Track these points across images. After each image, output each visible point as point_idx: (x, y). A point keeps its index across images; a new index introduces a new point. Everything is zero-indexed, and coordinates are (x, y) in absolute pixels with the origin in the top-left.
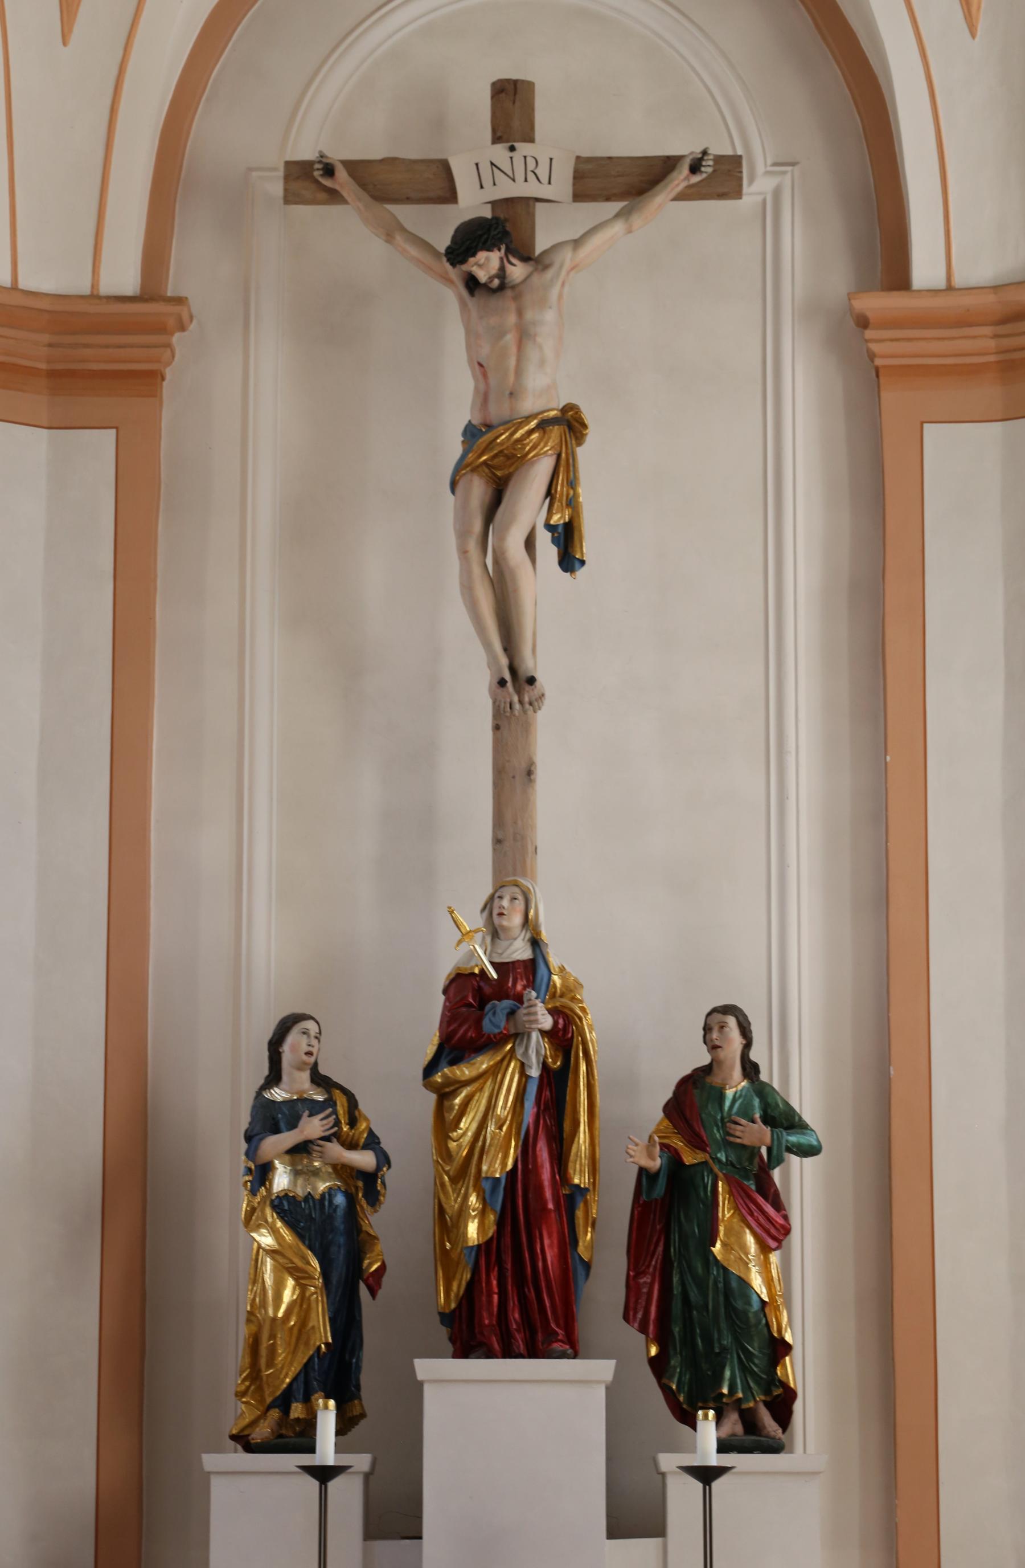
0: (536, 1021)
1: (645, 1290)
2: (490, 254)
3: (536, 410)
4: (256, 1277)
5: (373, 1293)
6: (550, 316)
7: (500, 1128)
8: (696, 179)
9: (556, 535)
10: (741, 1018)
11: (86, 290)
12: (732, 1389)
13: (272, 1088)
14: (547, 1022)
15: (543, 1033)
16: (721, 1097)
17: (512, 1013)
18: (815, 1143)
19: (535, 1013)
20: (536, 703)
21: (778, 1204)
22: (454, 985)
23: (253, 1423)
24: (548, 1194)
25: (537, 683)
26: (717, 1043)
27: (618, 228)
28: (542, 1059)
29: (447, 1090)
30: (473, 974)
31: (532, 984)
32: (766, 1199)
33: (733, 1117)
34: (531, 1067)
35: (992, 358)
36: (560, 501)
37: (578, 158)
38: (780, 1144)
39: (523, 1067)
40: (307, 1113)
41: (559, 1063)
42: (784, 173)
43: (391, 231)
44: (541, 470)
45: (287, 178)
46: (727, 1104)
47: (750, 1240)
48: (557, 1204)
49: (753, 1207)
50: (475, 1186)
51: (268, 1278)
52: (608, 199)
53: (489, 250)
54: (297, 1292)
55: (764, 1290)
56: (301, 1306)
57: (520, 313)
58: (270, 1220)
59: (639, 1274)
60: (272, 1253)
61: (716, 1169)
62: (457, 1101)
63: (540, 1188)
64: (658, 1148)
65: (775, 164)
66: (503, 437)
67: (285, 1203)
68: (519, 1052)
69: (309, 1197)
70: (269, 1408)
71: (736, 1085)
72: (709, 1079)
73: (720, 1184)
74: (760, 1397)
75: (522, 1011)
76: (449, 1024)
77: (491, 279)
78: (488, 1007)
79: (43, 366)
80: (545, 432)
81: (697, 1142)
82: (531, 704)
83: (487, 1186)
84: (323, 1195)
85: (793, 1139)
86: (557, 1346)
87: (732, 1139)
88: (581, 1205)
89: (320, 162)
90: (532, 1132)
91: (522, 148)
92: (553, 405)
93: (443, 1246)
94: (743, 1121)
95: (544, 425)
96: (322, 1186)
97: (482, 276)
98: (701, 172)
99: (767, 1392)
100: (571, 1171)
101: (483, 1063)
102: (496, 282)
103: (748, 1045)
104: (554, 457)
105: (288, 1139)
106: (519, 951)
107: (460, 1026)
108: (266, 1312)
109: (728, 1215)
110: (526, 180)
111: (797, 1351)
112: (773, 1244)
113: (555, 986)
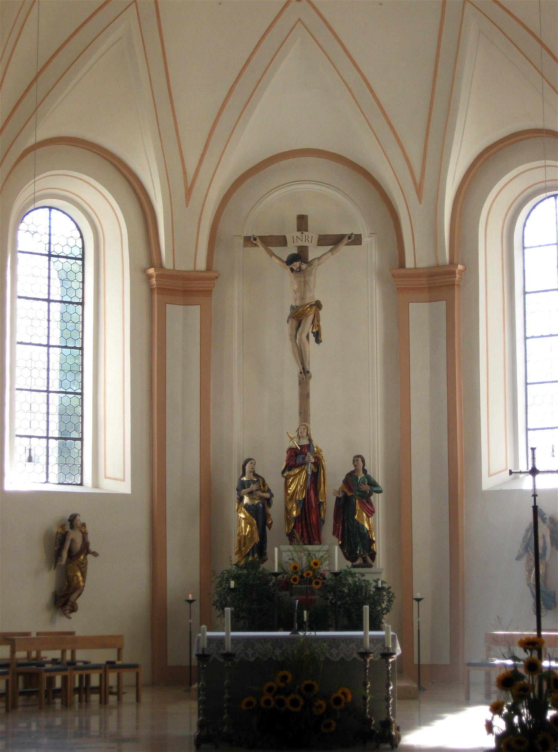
0: (310, 460)
1: (338, 527)
2: (297, 263)
3: (309, 302)
4: (240, 525)
5: (270, 528)
6: (312, 278)
7: (301, 488)
8: (350, 240)
9: (314, 334)
11: (193, 270)
12: (360, 552)
13: (243, 477)
14: (313, 460)
15: (312, 463)
16: (357, 478)
17: (304, 458)
18: (381, 490)
19: (310, 458)
20: (310, 377)
21: (371, 505)
22: (289, 451)
23: (239, 562)
24: (314, 504)
25: (310, 373)
26: (356, 465)
27: (330, 254)
28: (312, 470)
29: (288, 477)
30: (294, 448)
31: (309, 450)
32: (369, 504)
33: (360, 484)
34: (309, 472)
35: (426, 286)
36: (315, 325)
37: (319, 235)
38: (372, 491)
39: (307, 472)
40: (252, 484)
41: (316, 471)
42: (373, 236)
43: (272, 254)
44: (311, 318)
45: (245, 241)
46: (358, 481)
47: (365, 515)
48: (316, 506)
49: (365, 506)
50: (295, 502)
51: (243, 525)
52: (327, 245)
53: (297, 262)
54: (250, 529)
55: (368, 527)
56: (251, 532)
57: (305, 278)
58: (243, 510)
59: (336, 523)
60: (244, 519)
61: (356, 496)
62: (290, 480)
63: (311, 501)
64: (341, 492)
65: (370, 234)
66: (301, 310)
67: (247, 506)
68: (306, 468)
69: (253, 505)
70: (243, 558)
71: (361, 475)
72: (354, 474)
73: (357, 501)
74: (367, 554)
75: (307, 458)
76: (288, 461)
77: (297, 269)
78: (298, 457)
79: (182, 289)
80: (311, 308)
81: (351, 490)
82: (308, 378)
83: (298, 502)
84: (257, 504)
85: (375, 489)
86: (316, 542)
87: (360, 489)
88: (322, 506)
89: (253, 237)
90: (309, 488)
91: (305, 233)
92: (313, 301)
93: (287, 517)
94: (363, 485)
95: (311, 306)
96: (256, 502)
97: (295, 268)
98: (351, 239)
99: (369, 552)
100: (319, 497)
101: (297, 471)
102: (298, 269)
103: (364, 465)
104: (314, 315)
105: (247, 490)
106: (305, 442)
107: (291, 461)
108: (243, 534)
109: (359, 508)
110: (305, 241)
111: (377, 542)
112: (370, 515)
113: (315, 451)
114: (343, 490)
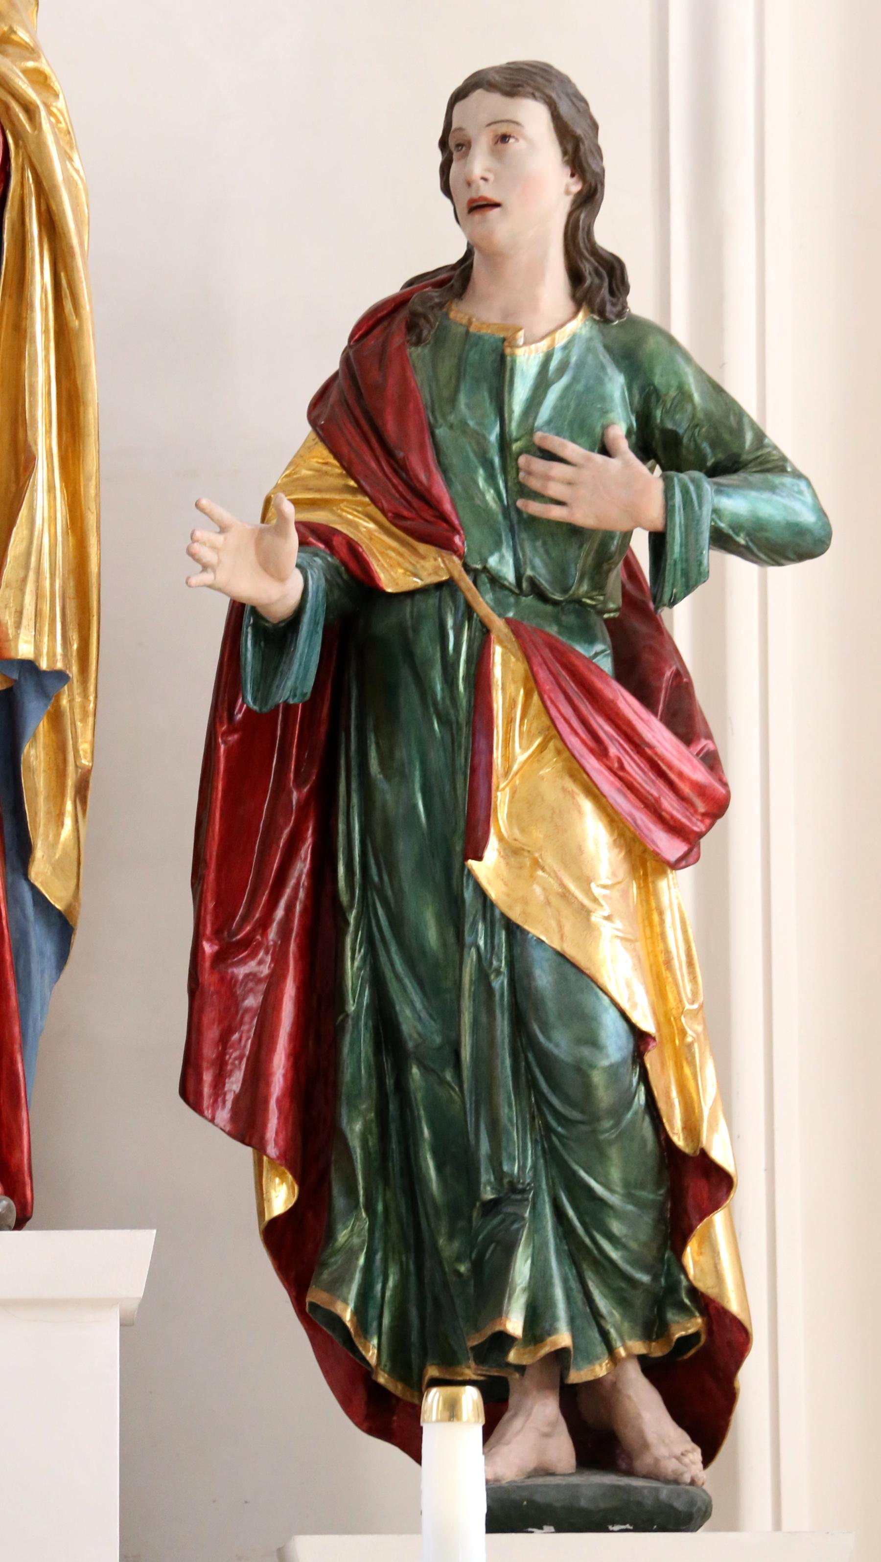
1: (252, 1001)
10: (565, 108)
18: (808, 518)
26: (488, 192)
32: (646, 697)
64: (294, 538)
73: (497, 652)
87: (534, 508)
94: (572, 450)
109: (521, 756)
114: (318, 517)
